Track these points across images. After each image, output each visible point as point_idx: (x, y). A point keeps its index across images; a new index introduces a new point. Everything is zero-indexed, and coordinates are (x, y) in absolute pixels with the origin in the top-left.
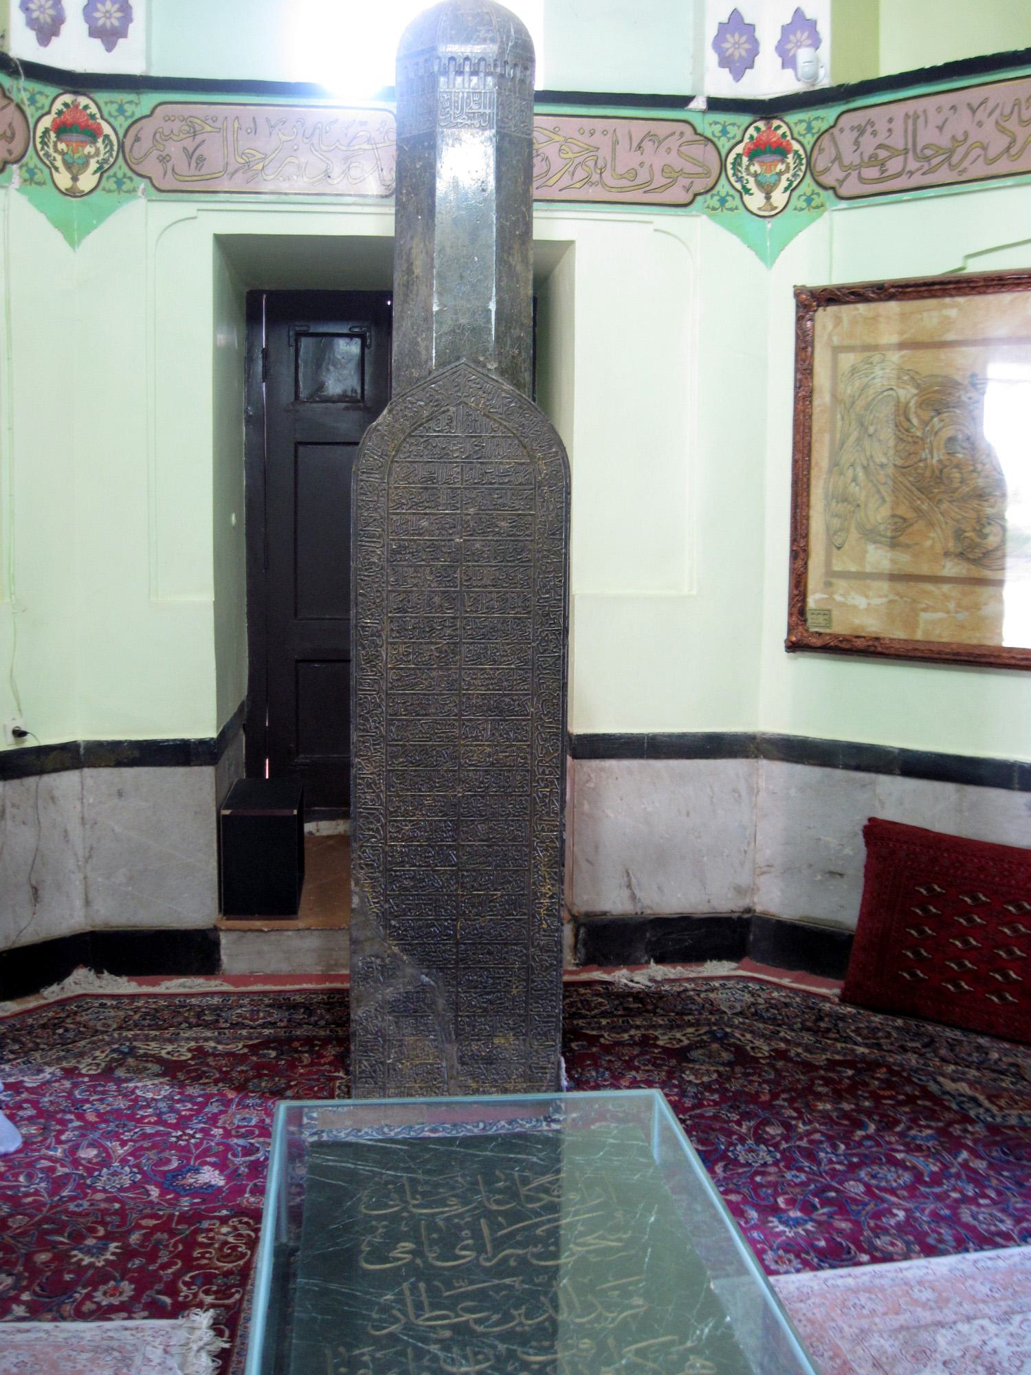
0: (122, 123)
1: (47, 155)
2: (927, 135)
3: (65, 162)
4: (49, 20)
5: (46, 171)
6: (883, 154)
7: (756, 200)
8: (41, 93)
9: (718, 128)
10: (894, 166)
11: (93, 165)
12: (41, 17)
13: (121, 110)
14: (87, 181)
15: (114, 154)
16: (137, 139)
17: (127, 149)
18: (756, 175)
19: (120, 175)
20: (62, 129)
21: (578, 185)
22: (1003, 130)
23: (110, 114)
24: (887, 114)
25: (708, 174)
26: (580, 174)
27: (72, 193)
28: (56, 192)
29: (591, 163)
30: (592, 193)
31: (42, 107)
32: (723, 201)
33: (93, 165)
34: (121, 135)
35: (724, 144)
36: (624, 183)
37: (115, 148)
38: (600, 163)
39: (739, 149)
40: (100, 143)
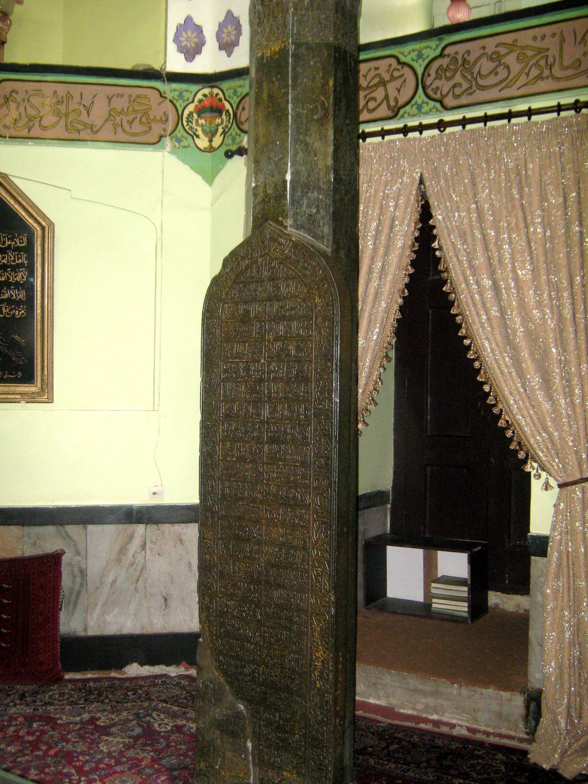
1: (191, 128)
3: (203, 131)
4: (193, 45)
5: (190, 138)
8: (187, 91)
11: (220, 130)
12: (189, 45)
15: (231, 121)
16: (243, 109)
17: (238, 117)
19: (234, 134)
20: (200, 111)
21: (532, 82)
23: (229, 97)
26: (534, 72)
28: (200, 152)
29: (542, 63)
31: (188, 99)
33: (220, 130)
34: (235, 108)
36: (570, 72)
37: (232, 117)
38: (550, 60)
40: (224, 117)
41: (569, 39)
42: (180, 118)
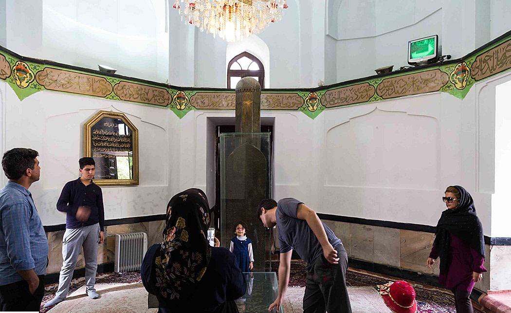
0: (189, 96)
2: (342, 96)
6: (334, 99)
7: (311, 108)
9: (303, 95)
10: (336, 101)
11: (184, 104)
13: (189, 94)
14: (183, 107)
16: (192, 99)
18: (311, 103)
20: (178, 98)
22: (356, 95)
24: (335, 92)
25: (301, 103)
26: (276, 104)
27: (180, 109)
30: (278, 108)
32: (304, 109)
33: (184, 104)
35: (304, 98)
39: (307, 98)
41: (285, 98)
42: (173, 99)
